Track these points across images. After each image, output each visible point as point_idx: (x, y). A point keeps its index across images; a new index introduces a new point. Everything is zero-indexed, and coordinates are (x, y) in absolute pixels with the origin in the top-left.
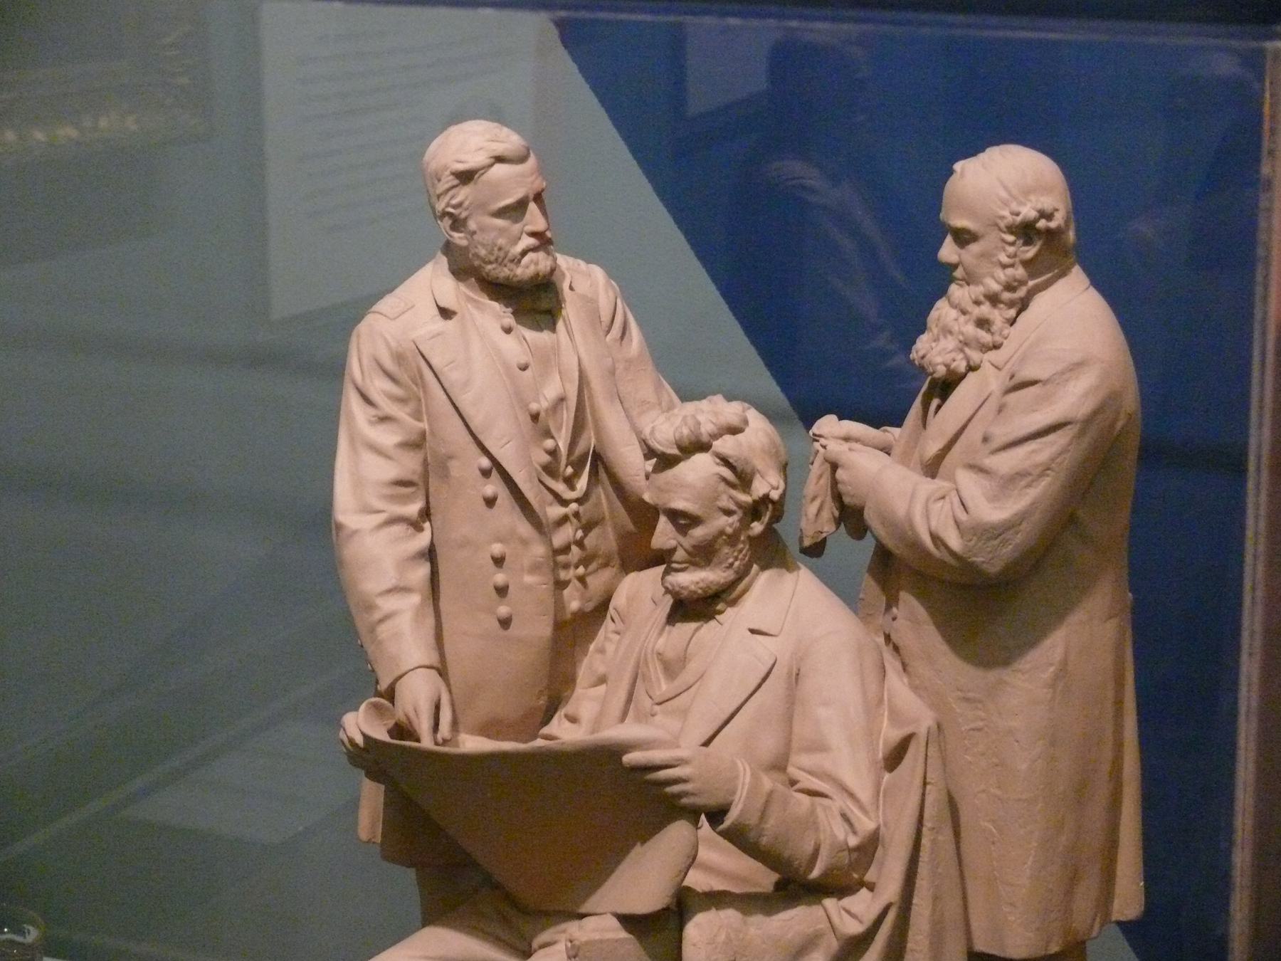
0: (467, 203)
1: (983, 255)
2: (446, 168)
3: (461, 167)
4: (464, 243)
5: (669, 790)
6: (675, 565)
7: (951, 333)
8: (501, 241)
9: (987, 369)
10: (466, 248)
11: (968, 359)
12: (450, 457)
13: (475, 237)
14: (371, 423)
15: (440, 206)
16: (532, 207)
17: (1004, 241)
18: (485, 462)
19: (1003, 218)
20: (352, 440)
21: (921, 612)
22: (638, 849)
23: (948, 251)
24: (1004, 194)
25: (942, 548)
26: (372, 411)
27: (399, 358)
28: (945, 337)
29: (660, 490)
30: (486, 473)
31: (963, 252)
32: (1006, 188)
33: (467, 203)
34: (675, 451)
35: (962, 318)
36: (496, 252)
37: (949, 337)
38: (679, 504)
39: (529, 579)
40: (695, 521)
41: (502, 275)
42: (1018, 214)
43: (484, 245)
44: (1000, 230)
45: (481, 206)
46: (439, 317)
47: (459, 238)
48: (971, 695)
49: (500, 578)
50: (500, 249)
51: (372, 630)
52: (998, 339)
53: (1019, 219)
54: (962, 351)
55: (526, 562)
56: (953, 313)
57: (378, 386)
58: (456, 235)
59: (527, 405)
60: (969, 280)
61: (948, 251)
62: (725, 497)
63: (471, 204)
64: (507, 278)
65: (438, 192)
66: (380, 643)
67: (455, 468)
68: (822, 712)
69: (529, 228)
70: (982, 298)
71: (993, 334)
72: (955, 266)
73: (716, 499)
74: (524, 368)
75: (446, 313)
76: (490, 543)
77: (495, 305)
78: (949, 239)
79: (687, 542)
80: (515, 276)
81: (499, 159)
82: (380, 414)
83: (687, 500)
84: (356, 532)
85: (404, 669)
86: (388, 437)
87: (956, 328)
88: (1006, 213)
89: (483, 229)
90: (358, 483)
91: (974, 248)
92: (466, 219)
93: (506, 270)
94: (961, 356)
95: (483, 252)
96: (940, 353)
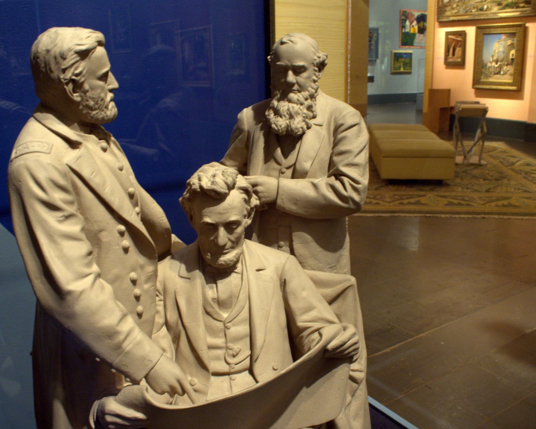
0: (85, 72)
1: (309, 78)
2: (70, 50)
3: (83, 48)
4: (78, 99)
5: (346, 352)
6: (225, 251)
7: (299, 114)
8: (102, 95)
9: (314, 127)
10: (78, 103)
11: (307, 124)
12: (101, 231)
13: (88, 94)
14: (60, 222)
15: (69, 75)
16: (110, 74)
17: (315, 70)
18: (122, 228)
19: (315, 60)
20: (51, 236)
21: (308, 237)
22: (305, 389)
23: (291, 77)
24: (313, 49)
25: (351, 203)
26: (59, 214)
27: (64, 175)
28: (297, 117)
29: (220, 214)
30: (122, 234)
31: (297, 77)
32: (314, 47)
33: (85, 72)
34: (227, 191)
35: (301, 107)
36: (100, 102)
37: (299, 116)
38: (233, 218)
39: (146, 286)
40: (237, 223)
41: (101, 116)
42: (319, 58)
43: (93, 99)
44: (314, 66)
45: (91, 73)
46: (69, 149)
47: (76, 97)
48: (332, 265)
49: (137, 291)
50: (102, 100)
51: (118, 347)
52: (315, 113)
53: (321, 59)
54: (304, 121)
55: (143, 278)
56: (296, 107)
57: (57, 197)
58: (75, 95)
59: (127, 190)
60: (302, 88)
61: (291, 77)
62: (245, 210)
63: (87, 72)
64: (103, 119)
65: (64, 67)
66: (128, 353)
67: (105, 237)
68: (304, 294)
69: (111, 87)
70: (308, 97)
71: (312, 112)
72: (293, 85)
73: (243, 211)
74: (121, 169)
75: (73, 144)
76: (129, 273)
77: (93, 137)
78: (290, 73)
79: (232, 237)
80: (107, 116)
81: (100, 43)
82: (66, 214)
83: (236, 214)
84: (82, 292)
85: (155, 361)
86: (73, 227)
87: (300, 112)
88: (316, 58)
89: (92, 88)
90: (67, 261)
91: (305, 75)
92: (83, 83)
93: (103, 113)
94: (304, 123)
95: (91, 103)
96: (298, 123)
